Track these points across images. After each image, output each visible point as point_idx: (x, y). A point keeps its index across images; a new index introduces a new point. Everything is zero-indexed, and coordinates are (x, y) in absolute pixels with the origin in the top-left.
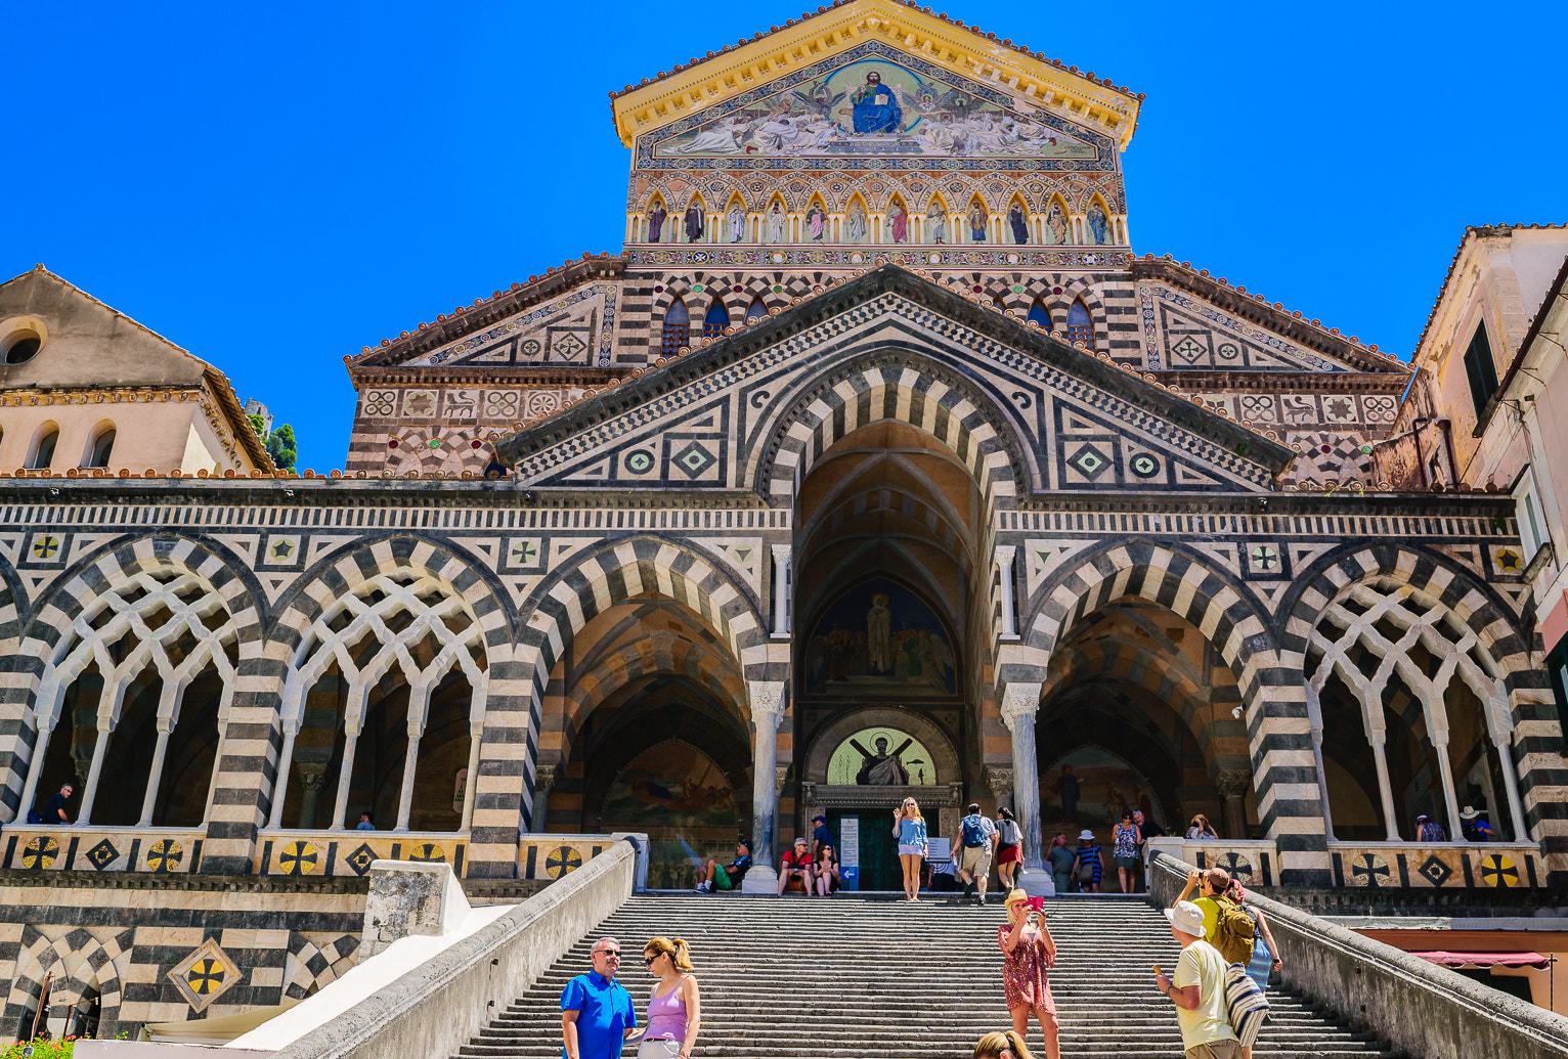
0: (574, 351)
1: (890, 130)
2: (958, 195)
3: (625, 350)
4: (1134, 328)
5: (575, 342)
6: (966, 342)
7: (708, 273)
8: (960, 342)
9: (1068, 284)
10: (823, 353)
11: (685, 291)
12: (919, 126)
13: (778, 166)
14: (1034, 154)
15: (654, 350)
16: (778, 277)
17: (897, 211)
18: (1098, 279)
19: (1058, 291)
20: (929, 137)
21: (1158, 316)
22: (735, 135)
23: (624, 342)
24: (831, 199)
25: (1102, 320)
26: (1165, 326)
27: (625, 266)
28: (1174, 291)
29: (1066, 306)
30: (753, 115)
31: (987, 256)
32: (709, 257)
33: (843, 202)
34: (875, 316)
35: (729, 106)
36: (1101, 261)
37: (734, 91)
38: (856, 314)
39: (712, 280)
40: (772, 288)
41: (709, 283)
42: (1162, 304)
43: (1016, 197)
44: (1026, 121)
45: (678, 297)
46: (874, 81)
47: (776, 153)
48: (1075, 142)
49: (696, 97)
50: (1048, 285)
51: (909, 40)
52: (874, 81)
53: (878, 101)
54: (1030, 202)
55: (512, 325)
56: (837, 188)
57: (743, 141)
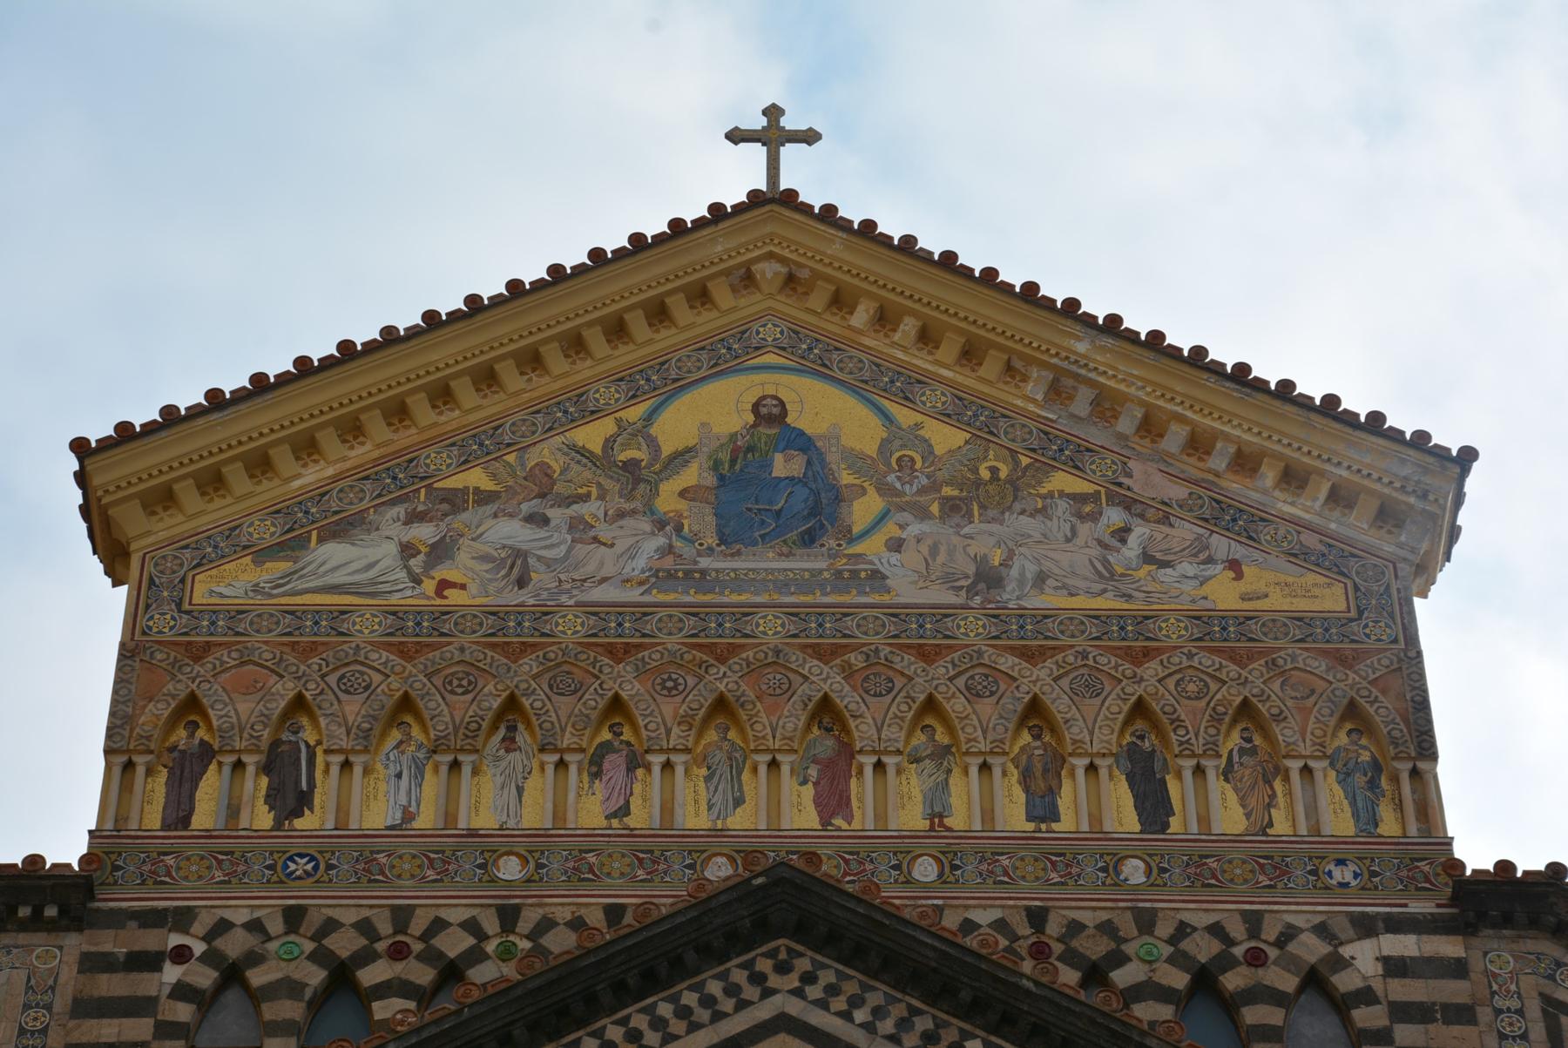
1: (809, 539)
2: (986, 707)
7: (321, 903)
9: (1282, 941)
11: (254, 959)
12: (890, 529)
13: (513, 635)
16: (508, 917)
17: (826, 746)
18: (1366, 927)
19: (1256, 959)
20: (912, 557)
22: (407, 550)
24: (661, 716)
30: (455, 501)
31: (1062, 859)
32: (321, 859)
33: (685, 721)
34: (742, 1005)
36: (1370, 879)
38: (690, 999)
39: (331, 926)
40: (490, 947)
41: (319, 936)
42: (1547, 1000)
43: (1140, 709)
44: (1165, 520)
45: (232, 974)
46: (770, 414)
47: (515, 597)
50: (1230, 942)
51: (861, 317)
52: (770, 414)
54: (1177, 723)
56: (672, 689)
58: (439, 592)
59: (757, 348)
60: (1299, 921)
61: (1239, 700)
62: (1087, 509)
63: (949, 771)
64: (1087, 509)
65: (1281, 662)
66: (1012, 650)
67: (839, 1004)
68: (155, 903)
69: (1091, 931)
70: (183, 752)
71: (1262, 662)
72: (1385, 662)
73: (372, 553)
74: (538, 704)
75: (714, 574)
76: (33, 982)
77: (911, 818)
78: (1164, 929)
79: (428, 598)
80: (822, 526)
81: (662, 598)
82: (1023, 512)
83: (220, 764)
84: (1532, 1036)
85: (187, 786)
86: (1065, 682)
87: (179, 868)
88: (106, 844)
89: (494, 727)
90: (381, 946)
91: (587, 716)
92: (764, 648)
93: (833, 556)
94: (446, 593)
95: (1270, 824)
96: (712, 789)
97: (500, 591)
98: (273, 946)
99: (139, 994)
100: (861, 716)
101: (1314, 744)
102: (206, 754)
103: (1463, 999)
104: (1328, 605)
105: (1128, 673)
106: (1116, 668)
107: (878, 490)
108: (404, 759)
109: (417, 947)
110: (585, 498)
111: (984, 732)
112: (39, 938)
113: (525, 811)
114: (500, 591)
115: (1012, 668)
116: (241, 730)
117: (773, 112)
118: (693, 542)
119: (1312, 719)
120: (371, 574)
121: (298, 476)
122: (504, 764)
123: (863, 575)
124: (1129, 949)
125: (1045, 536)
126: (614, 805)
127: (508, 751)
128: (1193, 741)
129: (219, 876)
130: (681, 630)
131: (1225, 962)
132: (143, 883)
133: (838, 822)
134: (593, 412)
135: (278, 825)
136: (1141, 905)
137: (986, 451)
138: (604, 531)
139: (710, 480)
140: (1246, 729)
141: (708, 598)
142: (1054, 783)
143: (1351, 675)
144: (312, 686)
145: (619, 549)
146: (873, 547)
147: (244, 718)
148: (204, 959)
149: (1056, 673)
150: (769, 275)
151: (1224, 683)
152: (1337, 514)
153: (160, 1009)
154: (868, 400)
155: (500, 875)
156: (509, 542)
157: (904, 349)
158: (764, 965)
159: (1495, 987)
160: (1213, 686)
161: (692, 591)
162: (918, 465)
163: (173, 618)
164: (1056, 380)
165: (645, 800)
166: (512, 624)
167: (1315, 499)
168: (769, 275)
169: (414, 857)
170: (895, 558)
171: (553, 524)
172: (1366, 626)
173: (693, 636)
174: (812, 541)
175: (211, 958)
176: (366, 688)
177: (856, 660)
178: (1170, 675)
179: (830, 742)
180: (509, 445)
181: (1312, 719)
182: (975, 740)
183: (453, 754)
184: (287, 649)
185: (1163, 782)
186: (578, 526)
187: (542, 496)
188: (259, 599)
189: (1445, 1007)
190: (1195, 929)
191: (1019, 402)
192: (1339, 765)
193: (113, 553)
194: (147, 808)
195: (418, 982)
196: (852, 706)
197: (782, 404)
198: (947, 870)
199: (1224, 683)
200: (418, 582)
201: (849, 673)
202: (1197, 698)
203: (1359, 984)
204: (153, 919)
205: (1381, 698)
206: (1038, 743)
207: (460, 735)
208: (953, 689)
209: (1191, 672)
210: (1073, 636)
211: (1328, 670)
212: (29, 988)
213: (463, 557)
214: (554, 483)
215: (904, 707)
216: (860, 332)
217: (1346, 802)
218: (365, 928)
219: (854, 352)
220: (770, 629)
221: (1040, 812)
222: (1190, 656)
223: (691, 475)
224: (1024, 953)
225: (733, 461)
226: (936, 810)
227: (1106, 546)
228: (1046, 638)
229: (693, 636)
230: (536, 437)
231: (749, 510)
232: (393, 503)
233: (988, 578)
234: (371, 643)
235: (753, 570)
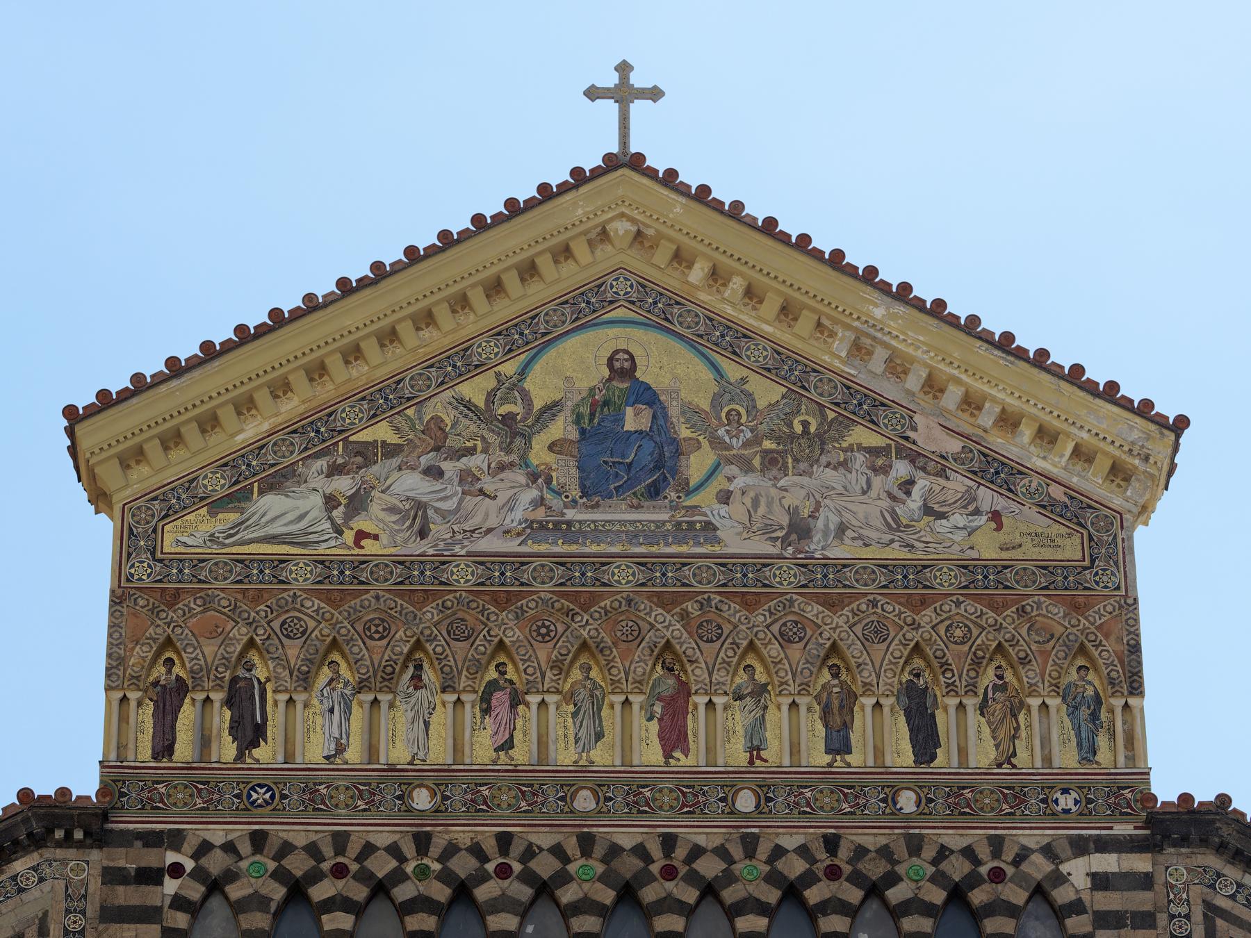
1: (654, 492)
2: (795, 651)
7: (280, 831)
9: (1018, 861)
11: (231, 876)
13: (418, 581)
14: (955, 552)
16: (422, 842)
18: (1081, 847)
19: (997, 876)
20: (738, 509)
22: (330, 501)
27: (105, 816)
28: (1233, 873)
29: (1012, 911)
30: (367, 454)
31: (850, 790)
35: (320, 434)
37: (325, 392)
39: (286, 848)
40: (409, 868)
44: (942, 473)
46: (622, 368)
48: (1041, 523)
49: (245, 406)
50: (977, 862)
51: (697, 274)
52: (622, 368)
53: (630, 423)
56: (545, 636)
57: (348, 517)
58: (357, 543)
59: (611, 302)
60: (1031, 843)
61: (994, 644)
62: (880, 462)
63: (765, 708)
64: (880, 462)
65: (1028, 608)
66: (816, 598)
68: (154, 826)
69: (873, 854)
70: (164, 687)
71: (1014, 609)
72: (1109, 608)
74: (439, 649)
75: (577, 526)
76: (70, 891)
77: (735, 754)
79: (349, 548)
80: (665, 479)
81: (536, 548)
82: (827, 466)
83: (193, 700)
85: (169, 718)
87: (170, 796)
88: (115, 776)
89: (405, 666)
90: (326, 866)
91: (478, 661)
92: (618, 597)
93: (674, 508)
94: (363, 543)
95: (1014, 754)
96: (578, 724)
97: (406, 541)
98: (244, 864)
99: (148, 903)
100: (696, 661)
101: (1051, 685)
102: (181, 689)
103: (1147, 908)
104: (1068, 555)
105: (909, 620)
106: (899, 615)
107: (711, 443)
108: (335, 695)
110: (471, 451)
111: (794, 675)
112: (71, 853)
113: (431, 743)
114: (406, 541)
115: (817, 616)
116: (209, 672)
117: (624, 69)
118: (560, 494)
119: (1051, 662)
120: (302, 525)
121: (242, 431)
122: (413, 700)
123: (698, 526)
124: (901, 869)
125: (845, 488)
126: (502, 737)
127: (416, 688)
128: (957, 683)
129: (199, 803)
130: (552, 579)
131: (973, 880)
132: (143, 808)
133: (677, 754)
134: (477, 366)
135: (240, 757)
136: (912, 831)
137: (799, 405)
138: (488, 484)
139: (574, 434)
140: (999, 667)
141: (573, 548)
142: (848, 719)
143: (1083, 621)
145: (501, 499)
146: (705, 499)
147: (209, 660)
149: (852, 621)
150: (621, 232)
151: (984, 629)
152: (1078, 468)
153: (164, 916)
155: (414, 805)
157: (733, 305)
159: (1172, 896)
160: (975, 632)
161: (560, 542)
162: (743, 420)
163: (149, 566)
164: (857, 338)
165: (525, 735)
166: (416, 573)
167: (1062, 456)
168: (621, 232)
169: (347, 789)
170: (724, 510)
171: (446, 477)
172: (1096, 574)
173: (562, 584)
174: (657, 493)
176: (303, 633)
177: (691, 606)
178: (942, 621)
180: (409, 399)
181: (1051, 662)
182: (786, 683)
184: (240, 596)
185: (933, 716)
186: (467, 477)
187: (437, 449)
188: (215, 549)
189: (1135, 914)
190: (952, 852)
191: (826, 358)
192: (1069, 700)
193: (99, 498)
194: (140, 737)
195: (355, 898)
196: (689, 652)
197: (632, 358)
198: (763, 801)
199: (984, 629)
200: (340, 533)
201: (685, 616)
202: (963, 643)
203: (1072, 896)
204: (153, 840)
205: (1104, 642)
206: (836, 682)
207: (379, 679)
208: (770, 635)
210: (866, 585)
211: (1064, 617)
212: (67, 896)
213: (375, 508)
214: (446, 437)
215: (730, 653)
216: (696, 287)
217: (1072, 733)
219: (691, 307)
220: (623, 577)
222: (958, 604)
223: (560, 428)
224: (821, 874)
225: (592, 415)
226: (755, 743)
227: (893, 498)
228: (845, 586)
229: (562, 584)
230: (431, 392)
231: (606, 462)
232: (317, 456)
233: (799, 530)
235: (609, 521)
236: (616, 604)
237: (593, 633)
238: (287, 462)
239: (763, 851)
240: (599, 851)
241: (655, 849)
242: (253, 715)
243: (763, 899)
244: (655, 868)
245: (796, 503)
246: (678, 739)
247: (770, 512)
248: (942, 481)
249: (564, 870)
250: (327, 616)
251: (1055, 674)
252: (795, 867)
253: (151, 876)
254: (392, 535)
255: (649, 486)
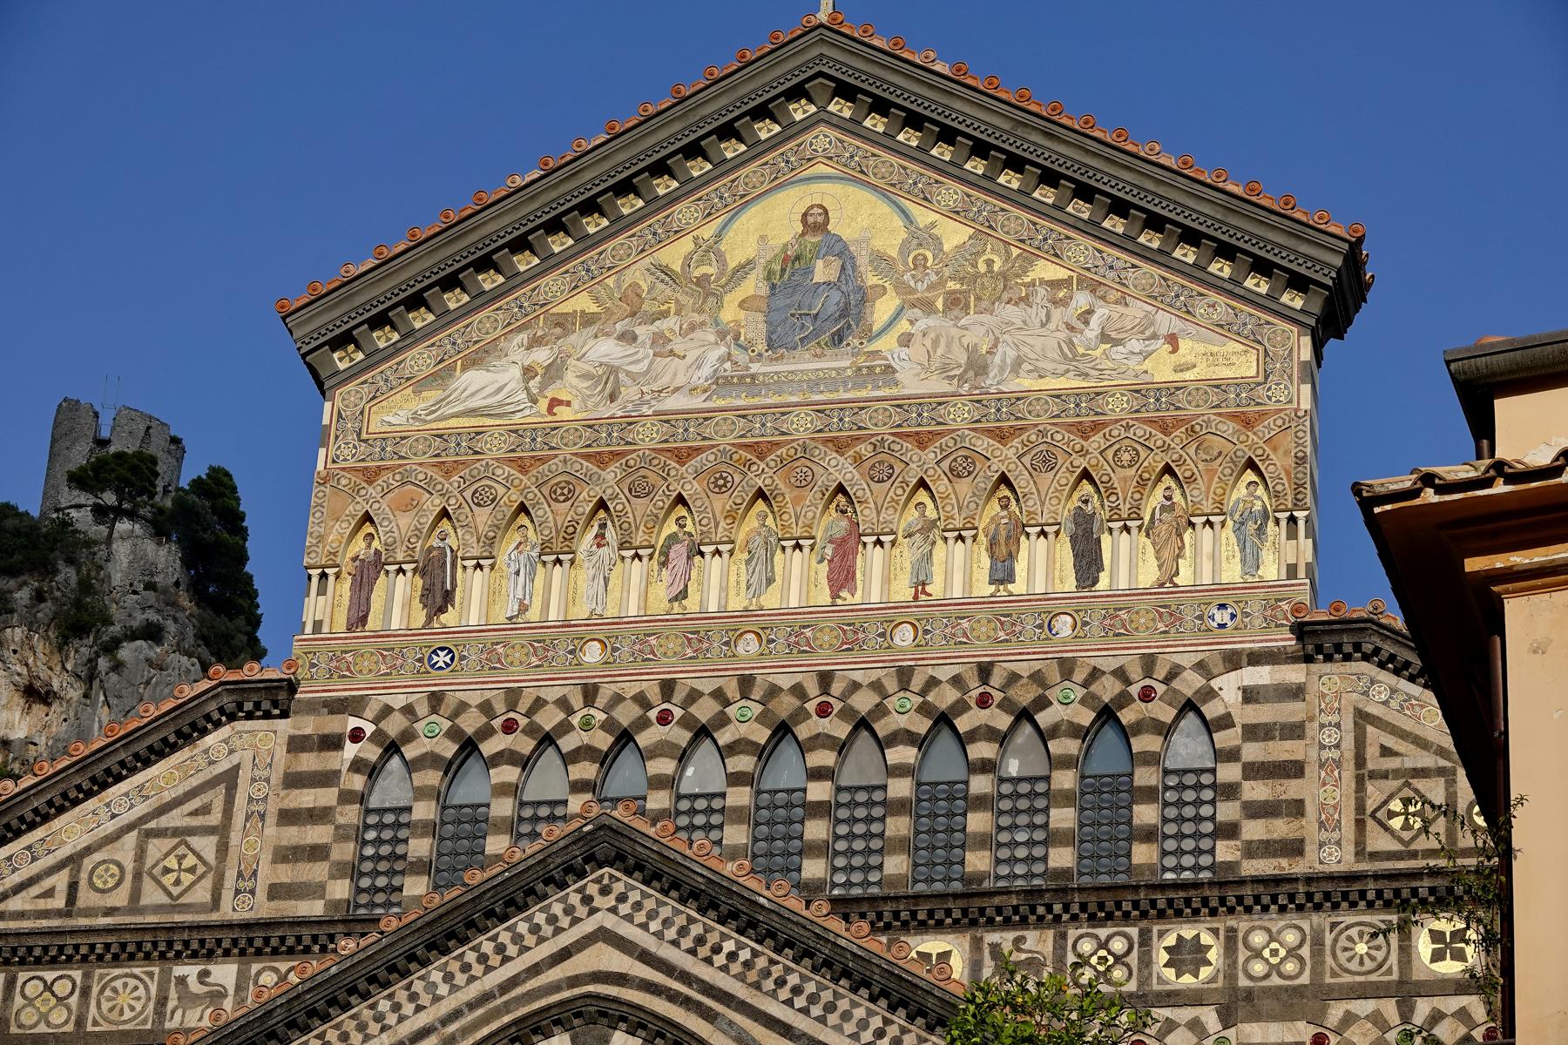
0: (187, 879)
1: (838, 339)
2: (964, 486)
3: (285, 874)
4: (1295, 769)
5: (190, 861)
6: (736, 968)
8: (724, 969)
10: (472, 1006)
12: (903, 326)
15: (340, 870)
16: (590, 693)
18: (1233, 661)
19: (1147, 695)
20: (917, 351)
21: (1349, 743)
22: (528, 372)
23: (287, 855)
25: (1232, 755)
26: (1360, 761)
30: (563, 323)
31: (1006, 616)
34: (575, 921)
38: (540, 918)
40: (575, 720)
43: (1086, 475)
46: (815, 222)
50: (1128, 682)
52: (815, 222)
54: (1111, 491)
55: (71, 830)
56: (720, 485)
58: (550, 411)
61: (1161, 466)
62: (1061, 295)
63: (934, 543)
65: (1197, 428)
66: (989, 432)
67: (640, 917)
72: (1279, 422)
73: (502, 378)
74: (619, 507)
78: (1080, 676)
81: (721, 403)
84: (1344, 745)
86: (1027, 460)
95: (1177, 573)
105: (1078, 448)
108: (522, 557)
109: (523, 721)
110: (664, 315)
111: (960, 509)
122: (595, 558)
123: (878, 370)
127: (599, 546)
131: (1123, 700)
135: (429, 620)
138: (678, 345)
139: (764, 290)
141: (756, 401)
142: (1013, 548)
144: (452, 501)
145: (689, 360)
146: (886, 344)
148: (373, 739)
154: (894, 203)
156: (604, 360)
158: (593, 889)
160: (1143, 454)
171: (640, 340)
174: (841, 341)
175: (378, 737)
179: (844, 523)
183: (557, 551)
185: (1099, 540)
186: (659, 339)
187: (633, 314)
188: (417, 425)
189: (1283, 726)
196: (860, 493)
200: (535, 402)
201: (858, 460)
203: (1221, 711)
204: (339, 707)
209: (1127, 442)
212: (254, 765)
213: (570, 377)
215: (900, 491)
218: (486, 708)
221: (1000, 576)
224: (973, 704)
225: (783, 270)
227: (1071, 328)
228: (1017, 419)
232: (520, 329)
233: (978, 366)
234: (497, 459)
236: (792, 452)
237: (768, 481)
238: (489, 338)
239: (917, 683)
240: (757, 694)
241: (812, 688)
242: (444, 583)
243: (913, 729)
244: (811, 706)
245: (975, 340)
246: (846, 579)
247: (949, 351)
248: (1121, 309)
249: (723, 713)
250: (516, 482)
251: (1219, 491)
252: (945, 697)
253: (331, 743)
254: (584, 401)
255: (833, 335)
